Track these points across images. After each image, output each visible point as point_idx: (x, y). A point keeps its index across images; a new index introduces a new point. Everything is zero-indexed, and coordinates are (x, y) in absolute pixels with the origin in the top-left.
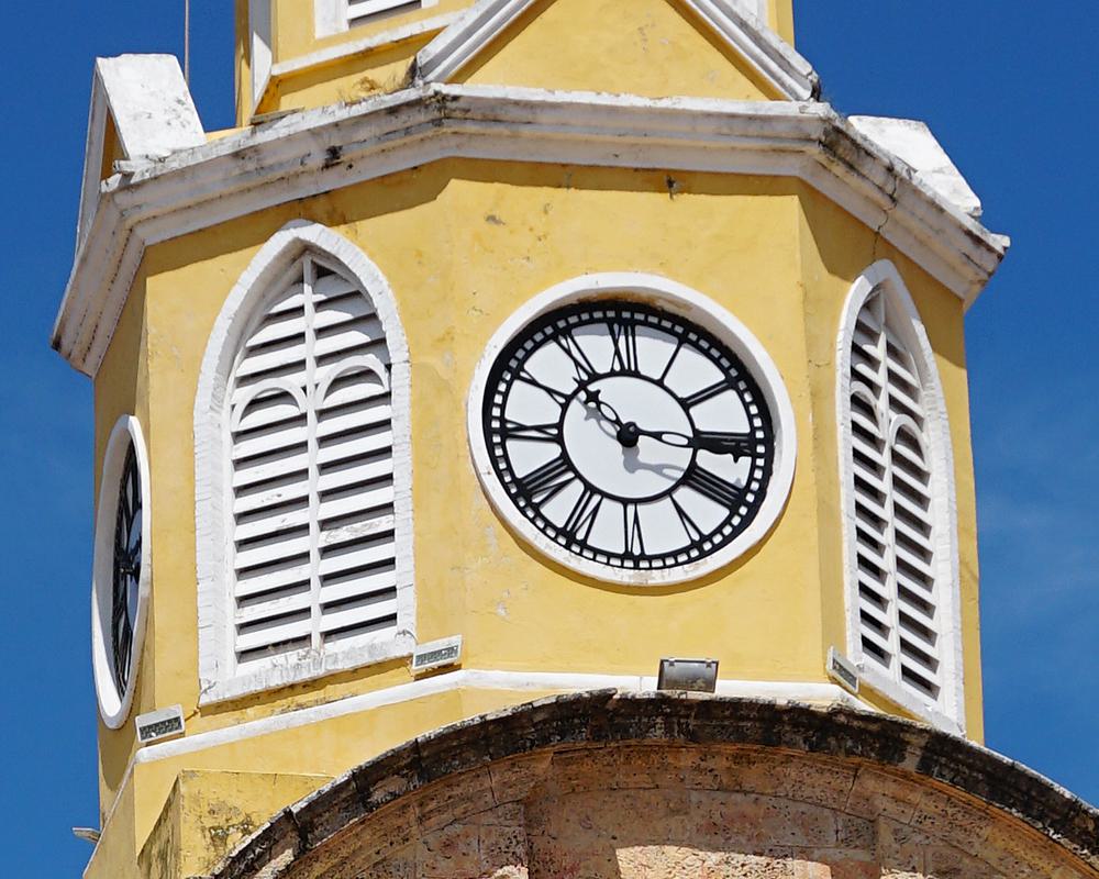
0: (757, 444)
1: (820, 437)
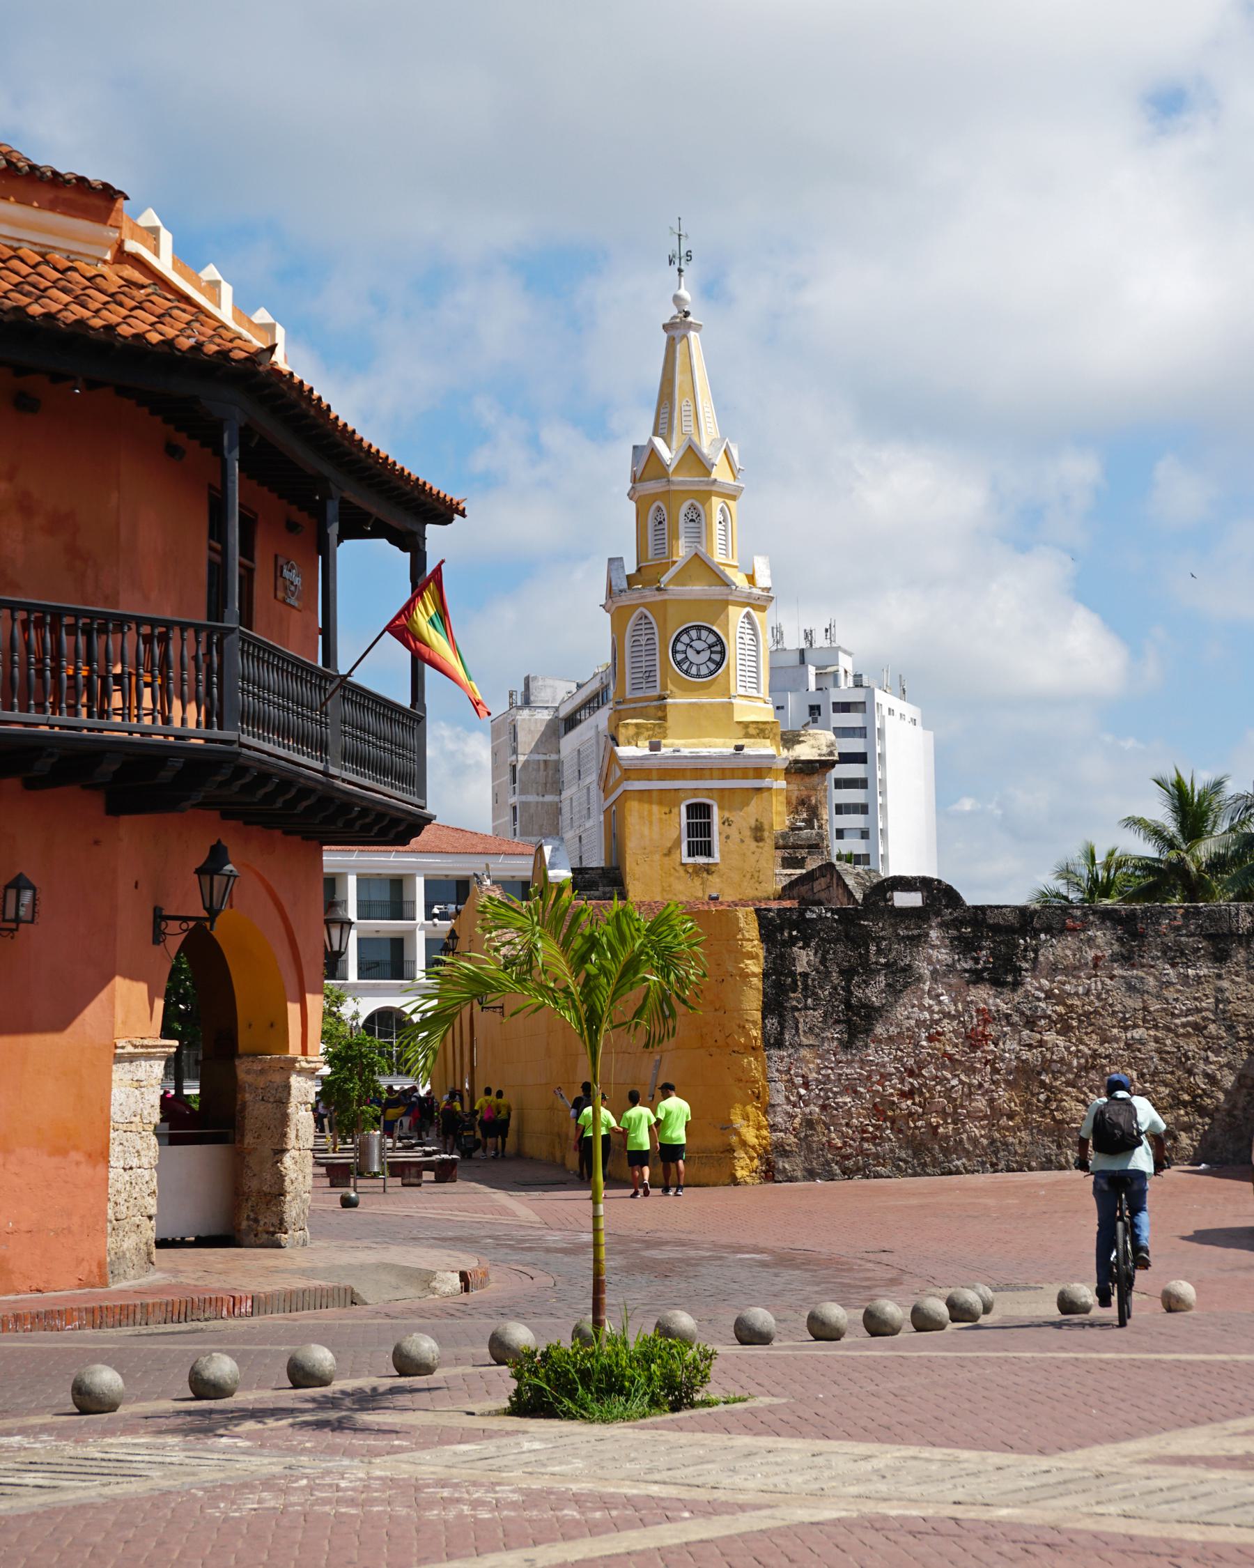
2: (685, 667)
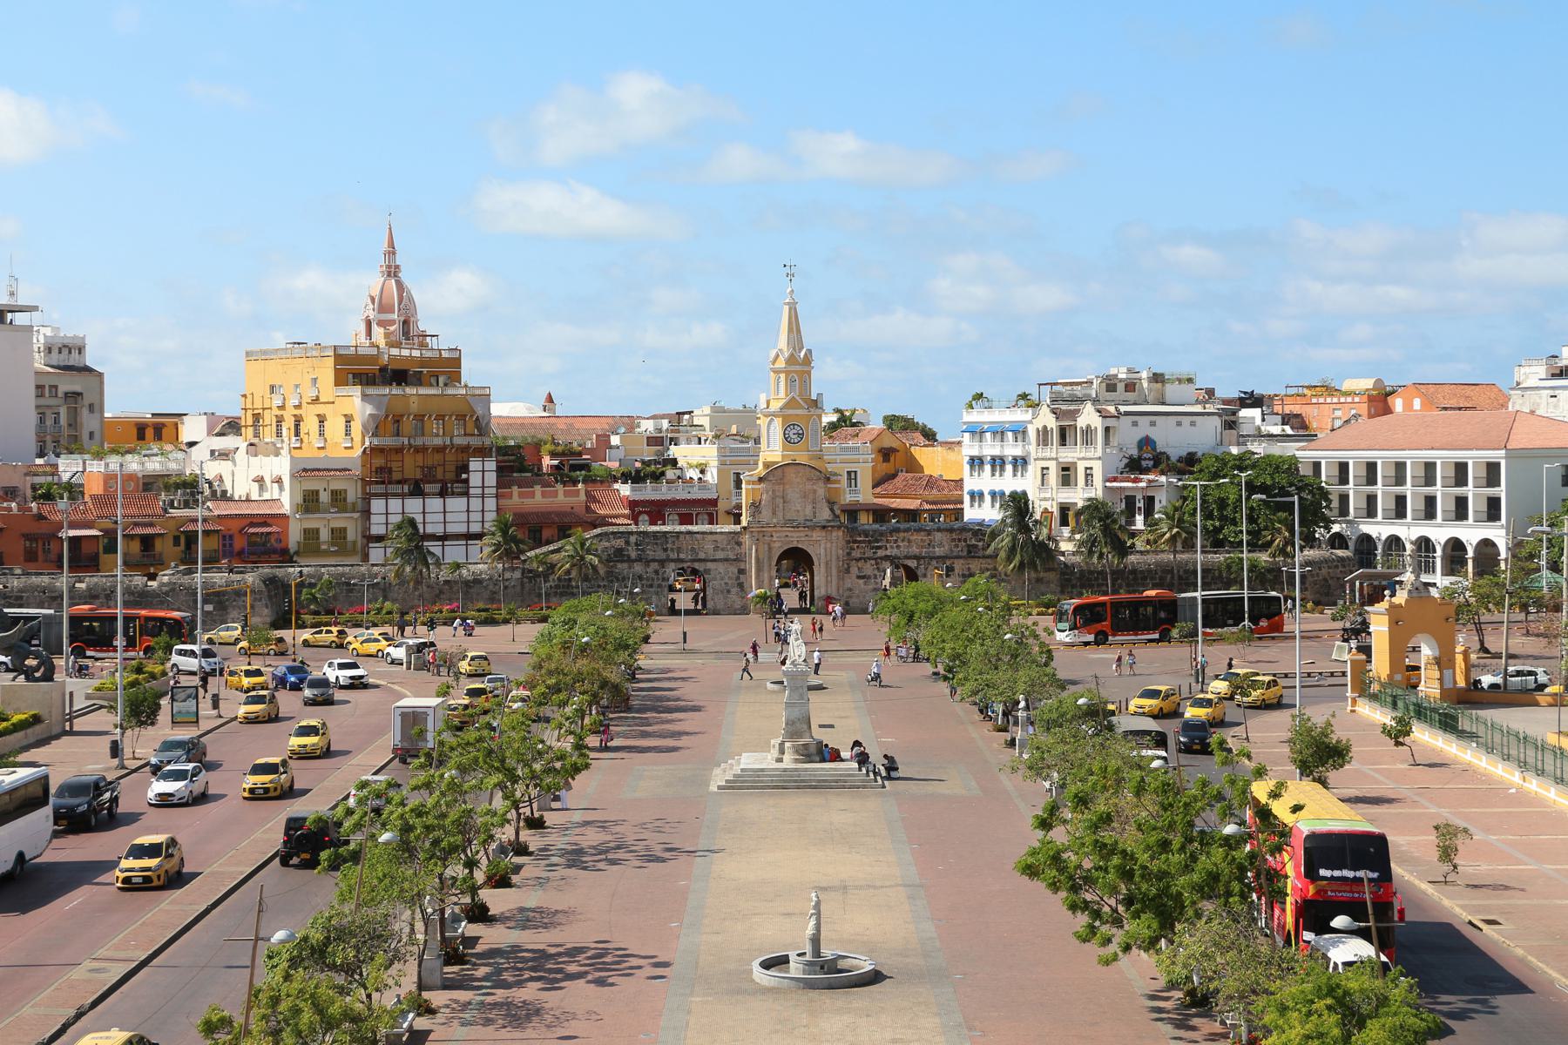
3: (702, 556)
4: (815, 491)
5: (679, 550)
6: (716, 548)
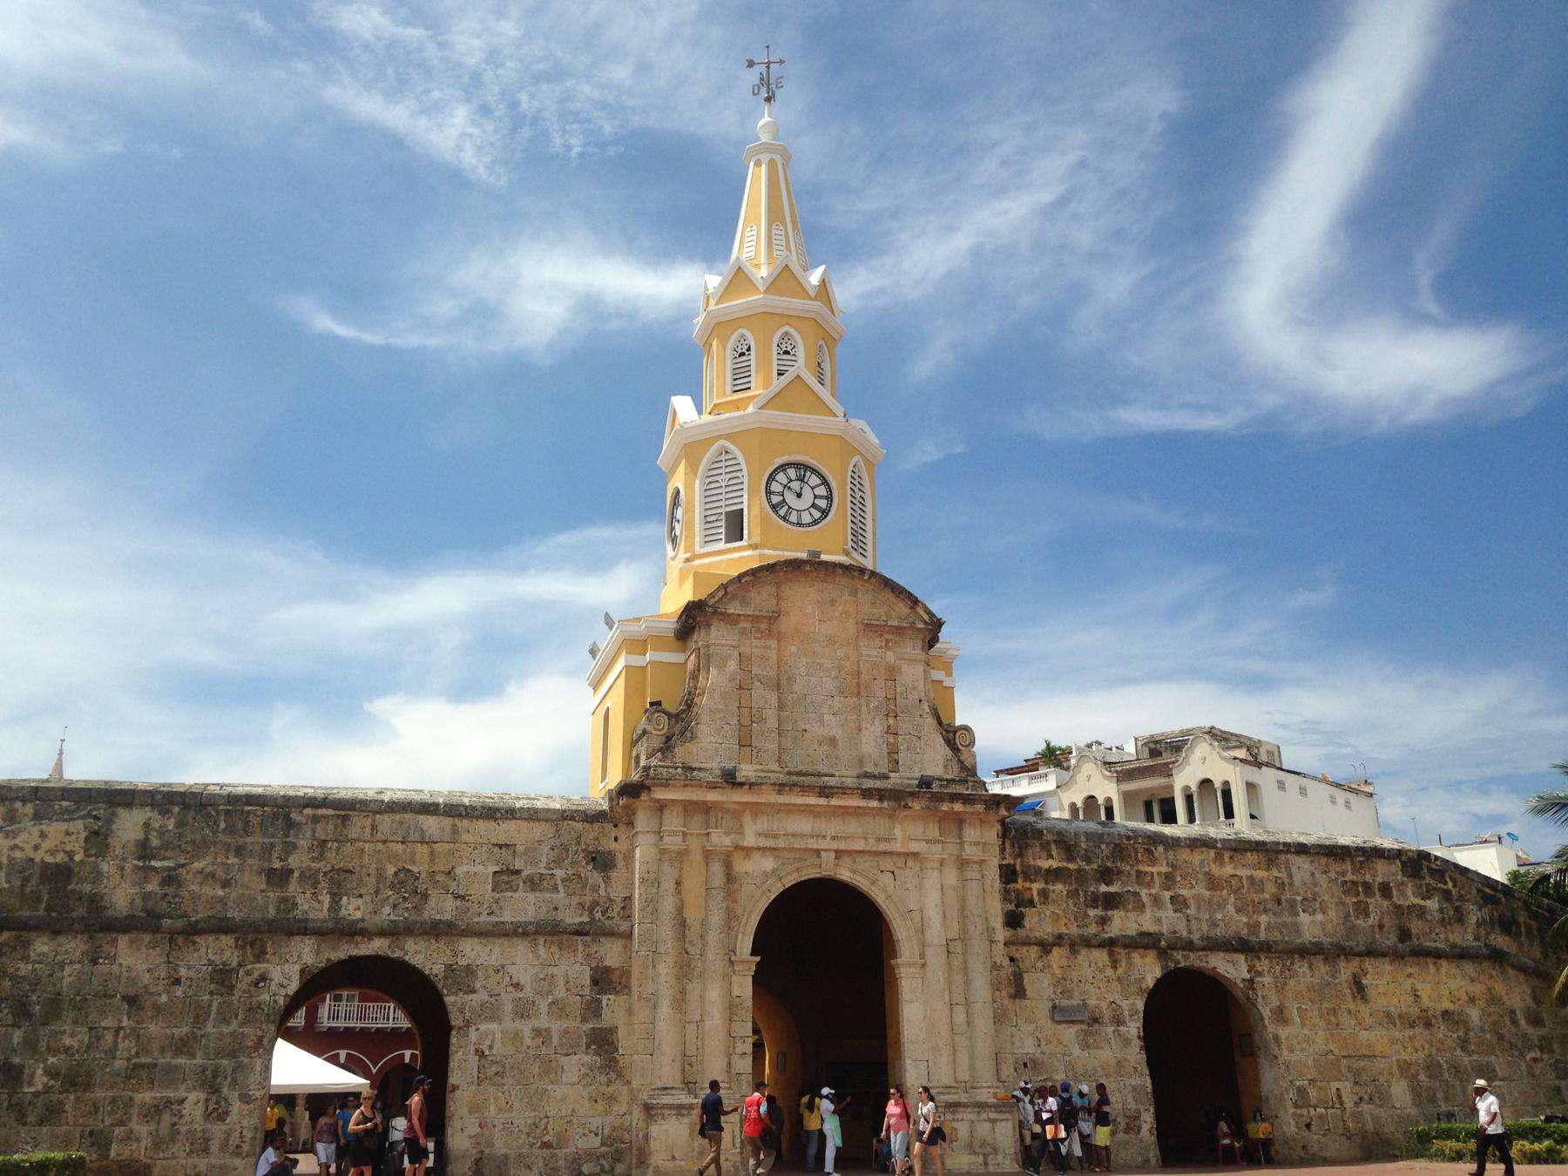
0: (829, 498)
1: (843, 499)
2: (782, 512)
3: (441, 907)
4: (892, 673)
5: (340, 882)
6: (506, 877)
